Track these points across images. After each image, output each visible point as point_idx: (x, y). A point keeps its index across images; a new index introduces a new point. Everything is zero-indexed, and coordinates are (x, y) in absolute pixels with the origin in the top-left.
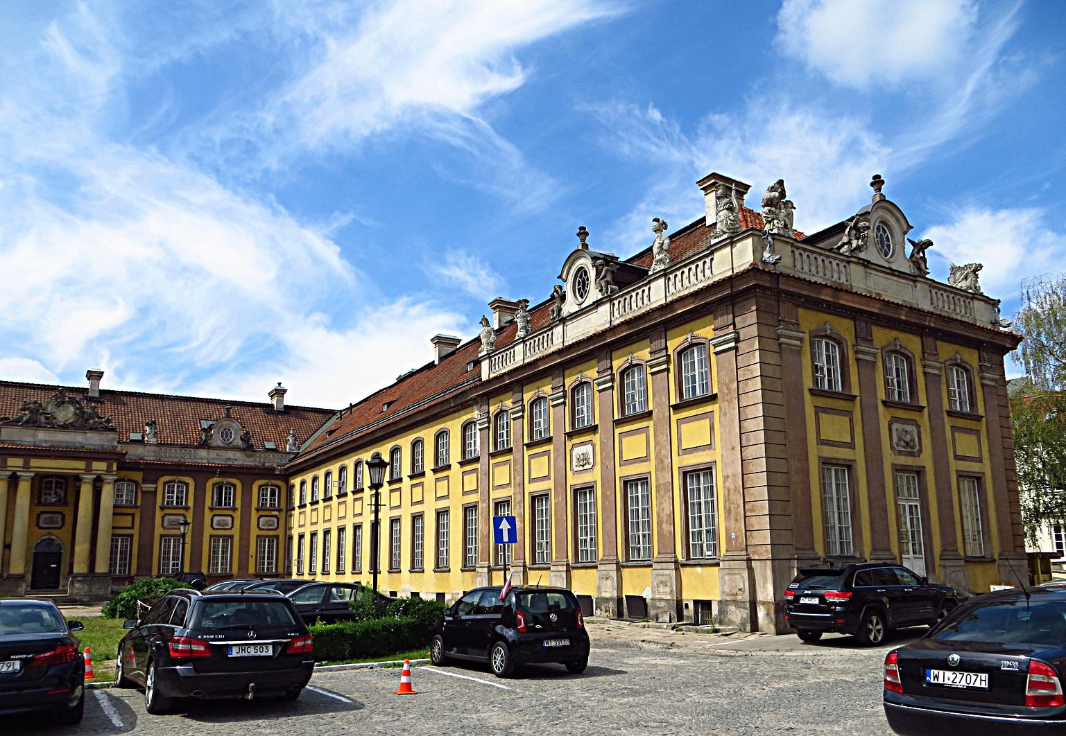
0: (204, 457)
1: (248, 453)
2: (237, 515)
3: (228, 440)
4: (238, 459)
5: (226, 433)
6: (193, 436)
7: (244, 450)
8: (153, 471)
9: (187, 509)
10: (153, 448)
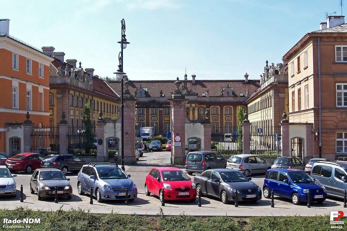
0: (222, 99)
1: (234, 98)
2: (233, 116)
3: (229, 94)
4: (231, 99)
5: (228, 93)
6: (219, 94)
7: (233, 97)
8: (209, 104)
9: (218, 115)
10: (208, 98)
